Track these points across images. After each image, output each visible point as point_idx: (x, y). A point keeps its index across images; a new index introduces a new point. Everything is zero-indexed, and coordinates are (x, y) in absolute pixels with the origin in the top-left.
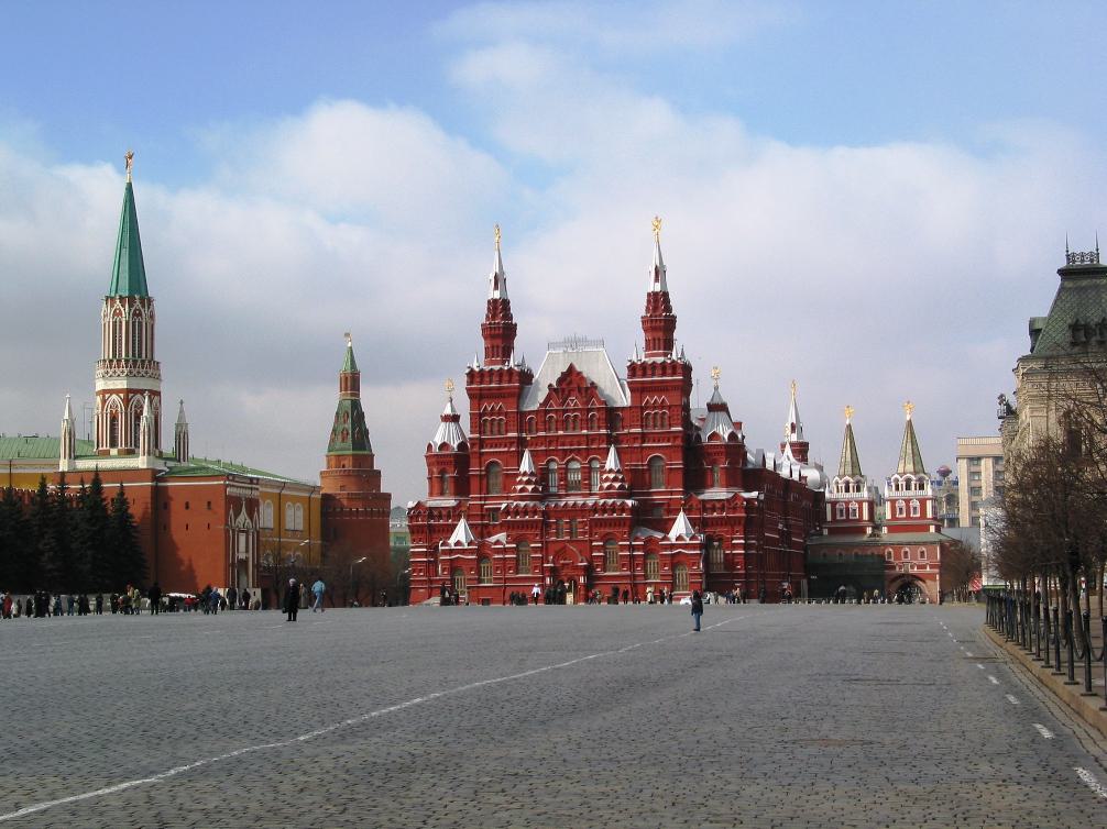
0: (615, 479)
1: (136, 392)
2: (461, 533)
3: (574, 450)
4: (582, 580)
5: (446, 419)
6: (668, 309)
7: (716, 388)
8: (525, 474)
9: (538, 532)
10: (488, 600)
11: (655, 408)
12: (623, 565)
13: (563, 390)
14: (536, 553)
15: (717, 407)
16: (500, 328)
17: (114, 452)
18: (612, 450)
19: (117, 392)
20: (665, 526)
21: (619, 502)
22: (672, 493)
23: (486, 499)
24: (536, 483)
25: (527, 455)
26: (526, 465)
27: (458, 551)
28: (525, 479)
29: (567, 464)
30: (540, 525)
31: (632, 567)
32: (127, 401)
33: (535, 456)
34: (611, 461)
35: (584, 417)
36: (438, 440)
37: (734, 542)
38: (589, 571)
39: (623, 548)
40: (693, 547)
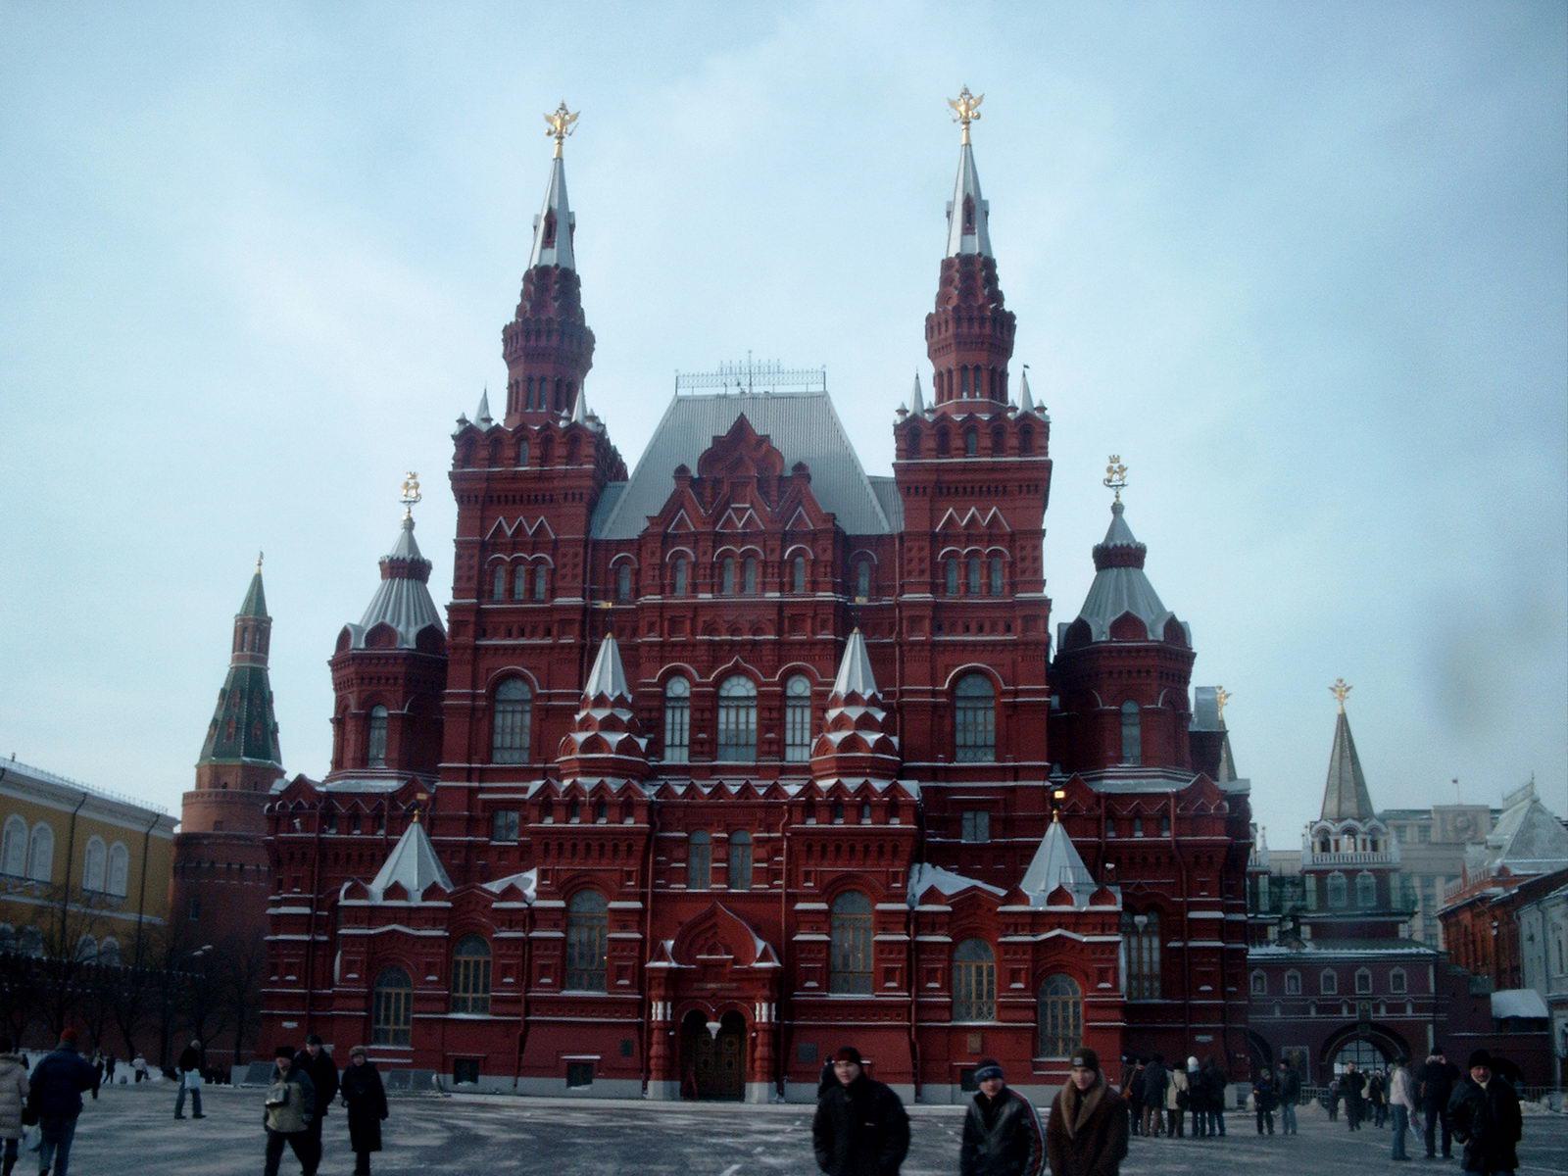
0: (866, 722)
2: (409, 864)
3: (743, 644)
4: (762, 1013)
6: (997, 297)
7: (1117, 509)
8: (600, 701)
9: (633, 866)
10: (474, 1062)
11: (970, 539)
12: (889, 974)
13: (717, 482)
14: (624, 928)
15: (1118, 556)
16: (549, 331)
18: (855, 645)
21: (879, 785)
22: (1016, 773)
23: (483, 775)
24: (629, 727)
25: (607, 653)
26: (604, 675)
27: (394, 915)
28: (600, 714)
29: (718, 683)
30: (639, 845)
31: (913, 979)
33: (631, 660)
34: (852, 673)
35: (775, 557)
37: (1193, 915)
38: (780, 987)
39: (885, 921)
40: (1102, 923)
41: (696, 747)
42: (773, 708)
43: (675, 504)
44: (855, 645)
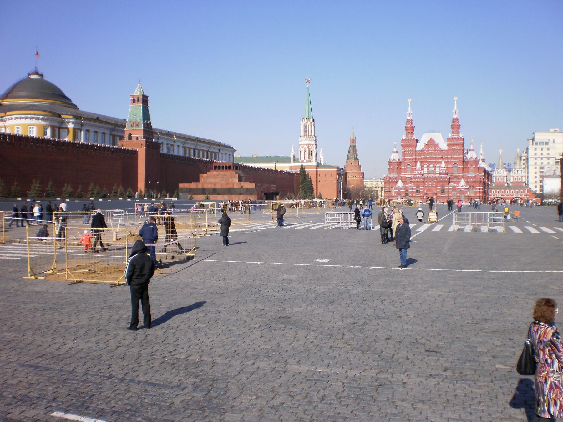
1: (311, 145)
2: (400, 184)
5: (393, 152)
17: (305, 161)
18: (443, 162)
19: (306, 145)
20: (458, 182)
26: (419, 165)
32: (308, 147)
33: (421, 162)
36: (392, 158)
41: (428, 172)
42: (435, 168)
43: (425, 147)
44: (443, 162)
